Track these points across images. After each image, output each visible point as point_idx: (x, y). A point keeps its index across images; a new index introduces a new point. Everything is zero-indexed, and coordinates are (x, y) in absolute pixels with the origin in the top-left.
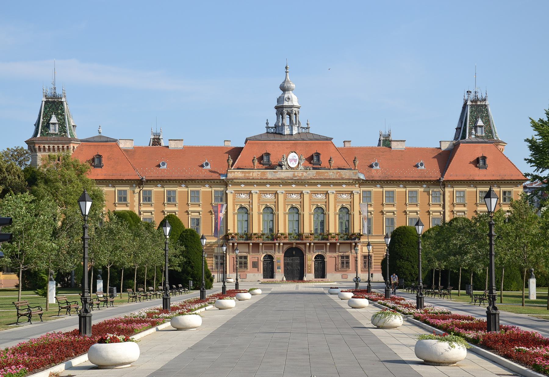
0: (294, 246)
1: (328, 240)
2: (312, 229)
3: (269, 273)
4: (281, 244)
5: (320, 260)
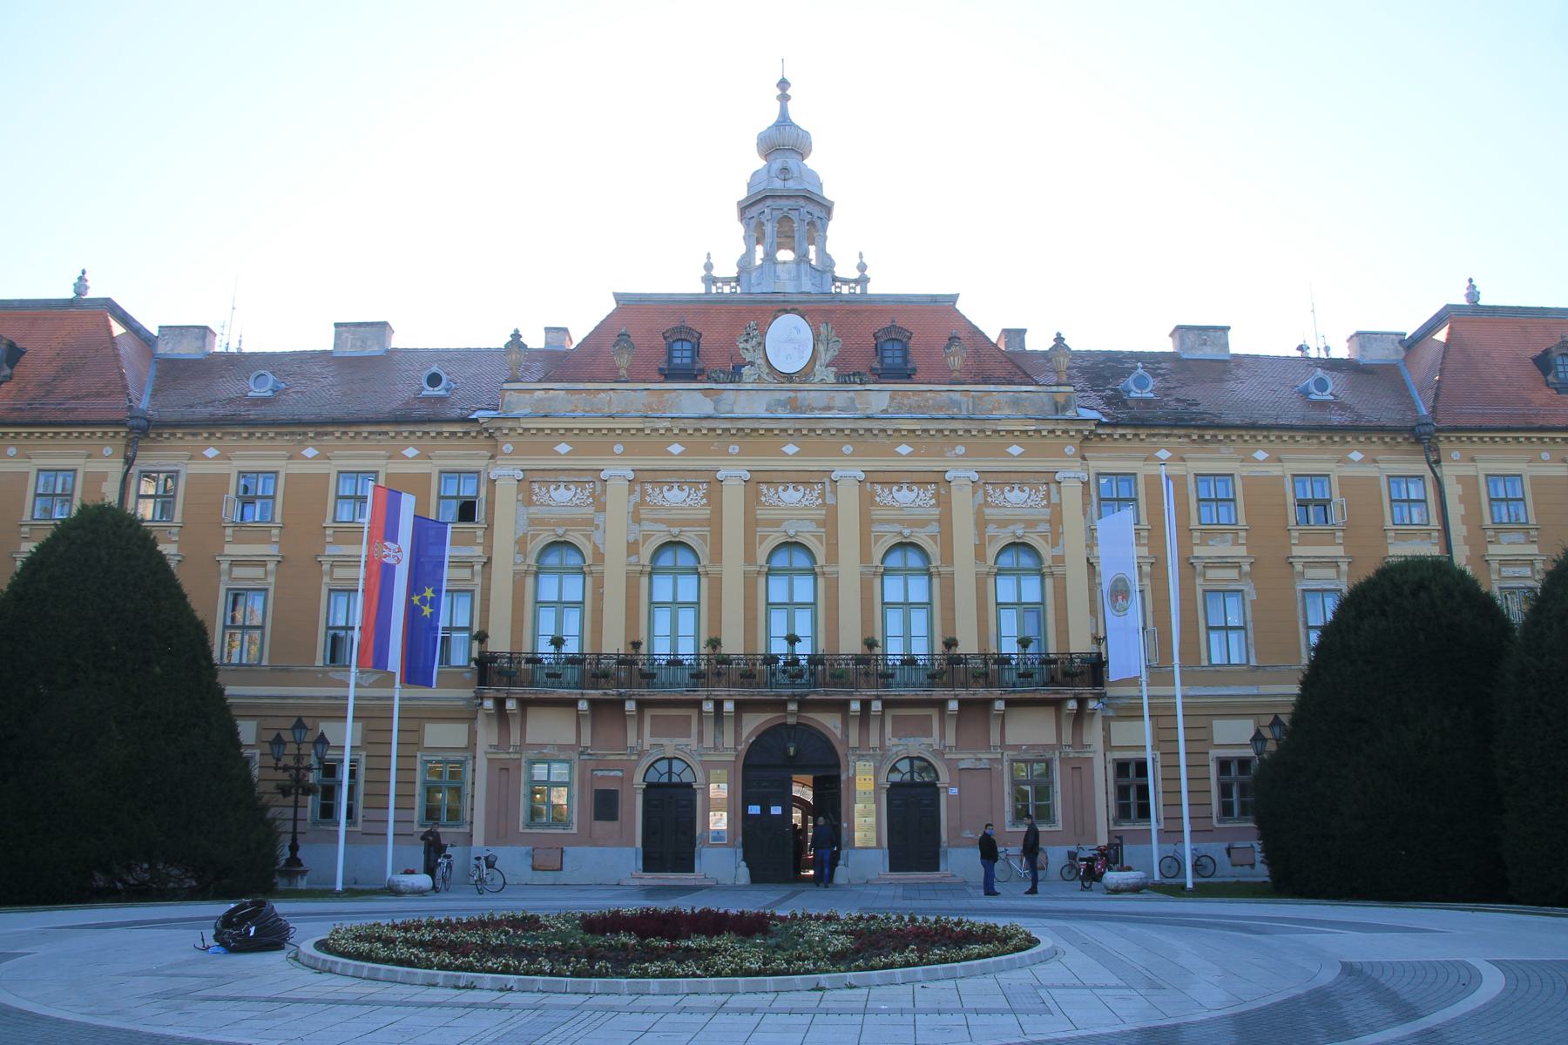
0: (791, 720)
1: (951, 685)
4: (729, 707)
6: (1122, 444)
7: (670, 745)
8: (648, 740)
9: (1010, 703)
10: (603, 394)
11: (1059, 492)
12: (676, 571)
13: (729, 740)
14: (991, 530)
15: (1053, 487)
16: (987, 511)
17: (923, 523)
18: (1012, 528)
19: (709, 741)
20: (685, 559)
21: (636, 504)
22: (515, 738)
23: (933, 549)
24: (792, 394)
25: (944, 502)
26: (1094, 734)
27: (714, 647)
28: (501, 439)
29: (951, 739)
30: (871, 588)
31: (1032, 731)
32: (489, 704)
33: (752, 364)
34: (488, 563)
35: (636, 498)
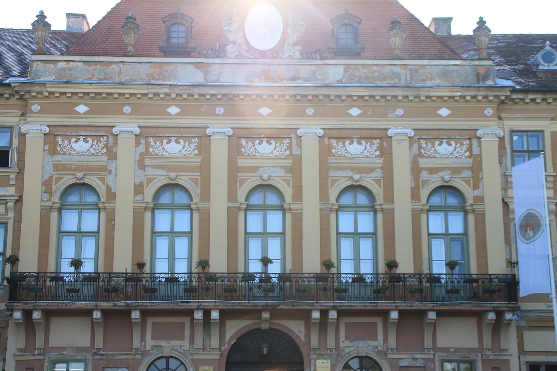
0: (265, 326)
1: (393, 298)
4: (215, 315)
6: (532, 107)
7: (168, 346)
8: (150, 343)
9: (440, 314)
10: (114, 66)
11: (480, 145)
12: (173, 208)
13: (215, 342)
14: (424, 175)
15: (475, 141)
16: (421, 160)
17: (369, 170)
18: (441, 174)
19: (199, 343)
20: (180, 198)
21: (141, 155)
22: (39, 342)
23: (378, 191)
24: (266, 67)
25: (386, 153)
26: (510, 342)
27: (204, 268)
28: (30, 101)
29: (392, 342)
30: (328, 221)
32: (18, 315)
33: (234, 43)
34: (19, 201)
35: (141, 149)
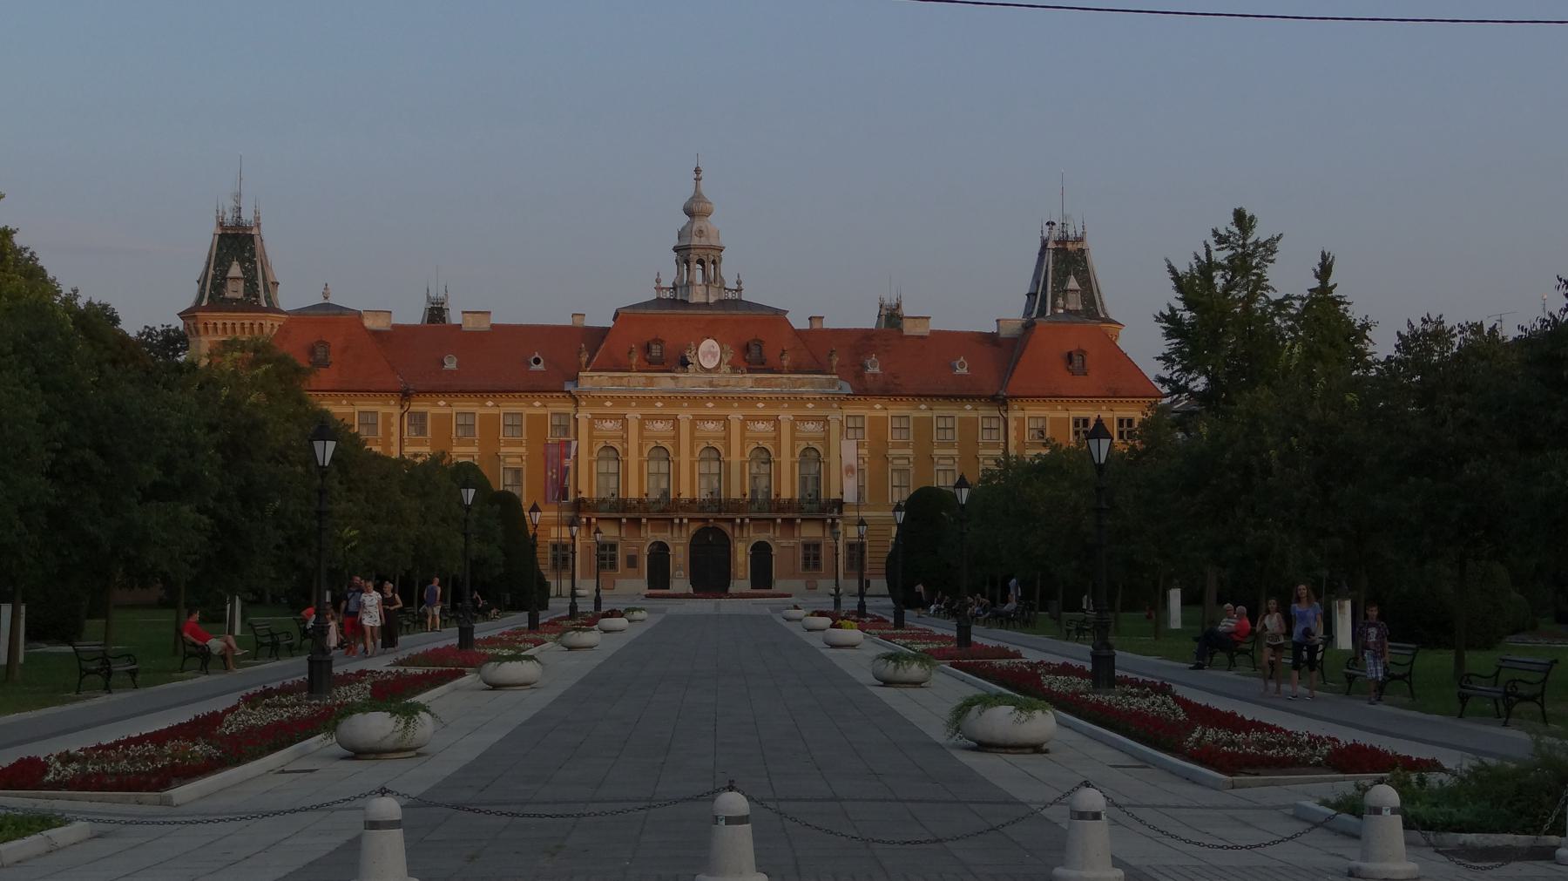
2: (748, 491)
3: (659, 575)
5: (761, 553)
13: (684, 534)
31: (811, 532)
